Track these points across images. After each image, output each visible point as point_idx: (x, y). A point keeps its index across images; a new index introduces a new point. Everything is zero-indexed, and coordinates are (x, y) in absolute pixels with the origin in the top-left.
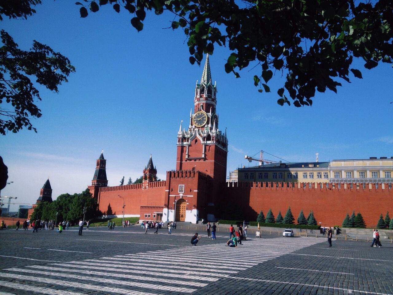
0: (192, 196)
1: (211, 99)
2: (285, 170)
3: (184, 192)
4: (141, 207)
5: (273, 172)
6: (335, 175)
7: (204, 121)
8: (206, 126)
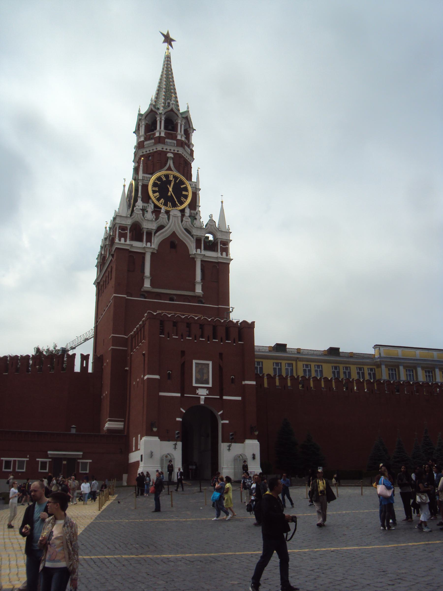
0: (239, 398)
1: (190, 151)
2: (298, 358)
3: (210, 385)
5: (272, 361)
6: (389, 374)
7: (183, 199)
8: (187, 211)
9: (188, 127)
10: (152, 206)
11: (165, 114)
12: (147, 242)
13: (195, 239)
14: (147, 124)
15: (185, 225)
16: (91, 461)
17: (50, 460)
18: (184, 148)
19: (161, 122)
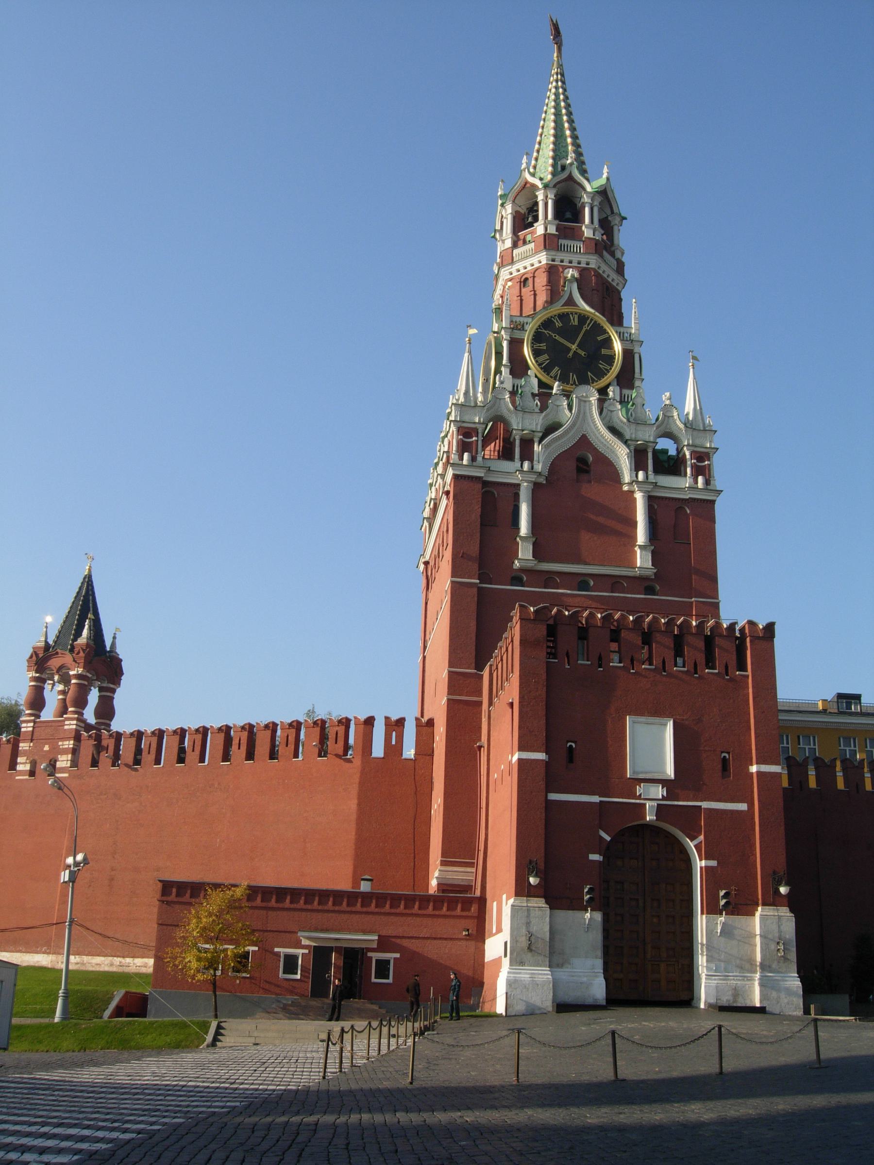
0: (743, 807)
4: (167, 886)
7: (602, 365)
9: (609, 212)
10: (535, 382)
11: (555, 186)
12: (522, 460)
13: (632, 448)
14: (517, 212)
15: (608, 418)
16: (398, 955)
17: (306, 951)
18: (601, 256)
19: (546, 204)
